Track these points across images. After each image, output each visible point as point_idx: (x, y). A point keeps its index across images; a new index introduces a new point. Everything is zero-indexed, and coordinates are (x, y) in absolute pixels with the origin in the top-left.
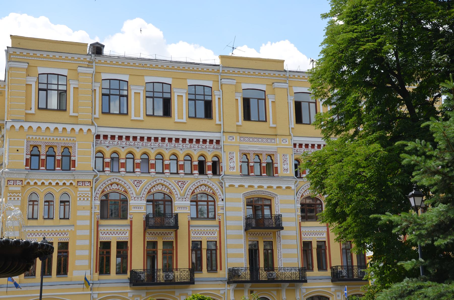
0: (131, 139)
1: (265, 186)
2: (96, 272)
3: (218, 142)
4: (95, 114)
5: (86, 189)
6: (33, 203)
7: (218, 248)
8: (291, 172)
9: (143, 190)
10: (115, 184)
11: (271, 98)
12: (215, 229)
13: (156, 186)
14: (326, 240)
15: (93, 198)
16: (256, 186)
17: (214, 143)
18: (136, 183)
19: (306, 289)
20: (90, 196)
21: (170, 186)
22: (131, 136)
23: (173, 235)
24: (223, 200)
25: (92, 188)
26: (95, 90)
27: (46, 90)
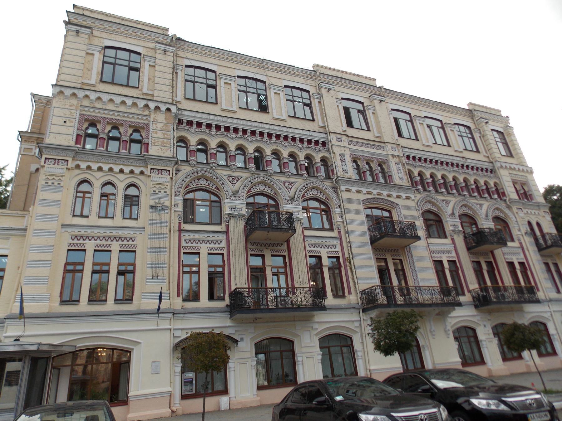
0: (222, 129)
1: (385, 193)
2: (178, 296)
3: (324, 144)
4: (176, 97)
6: (84, 196)
7: (342, 265)
8: (406, 182)
9: (242, 187)
10: (203, 179)
11: (371, 109)
12: (335, 242)
13: (257, 185)
14: (456, 259)
16: (375, 192)
17: (320, 145)
18: (231, 179)
20: (169, 187)
21: (275, 185)
23: (285, 247)
24: (339, 206)
25: (171, 178)
26: (176, 73)
27: (114, 64)
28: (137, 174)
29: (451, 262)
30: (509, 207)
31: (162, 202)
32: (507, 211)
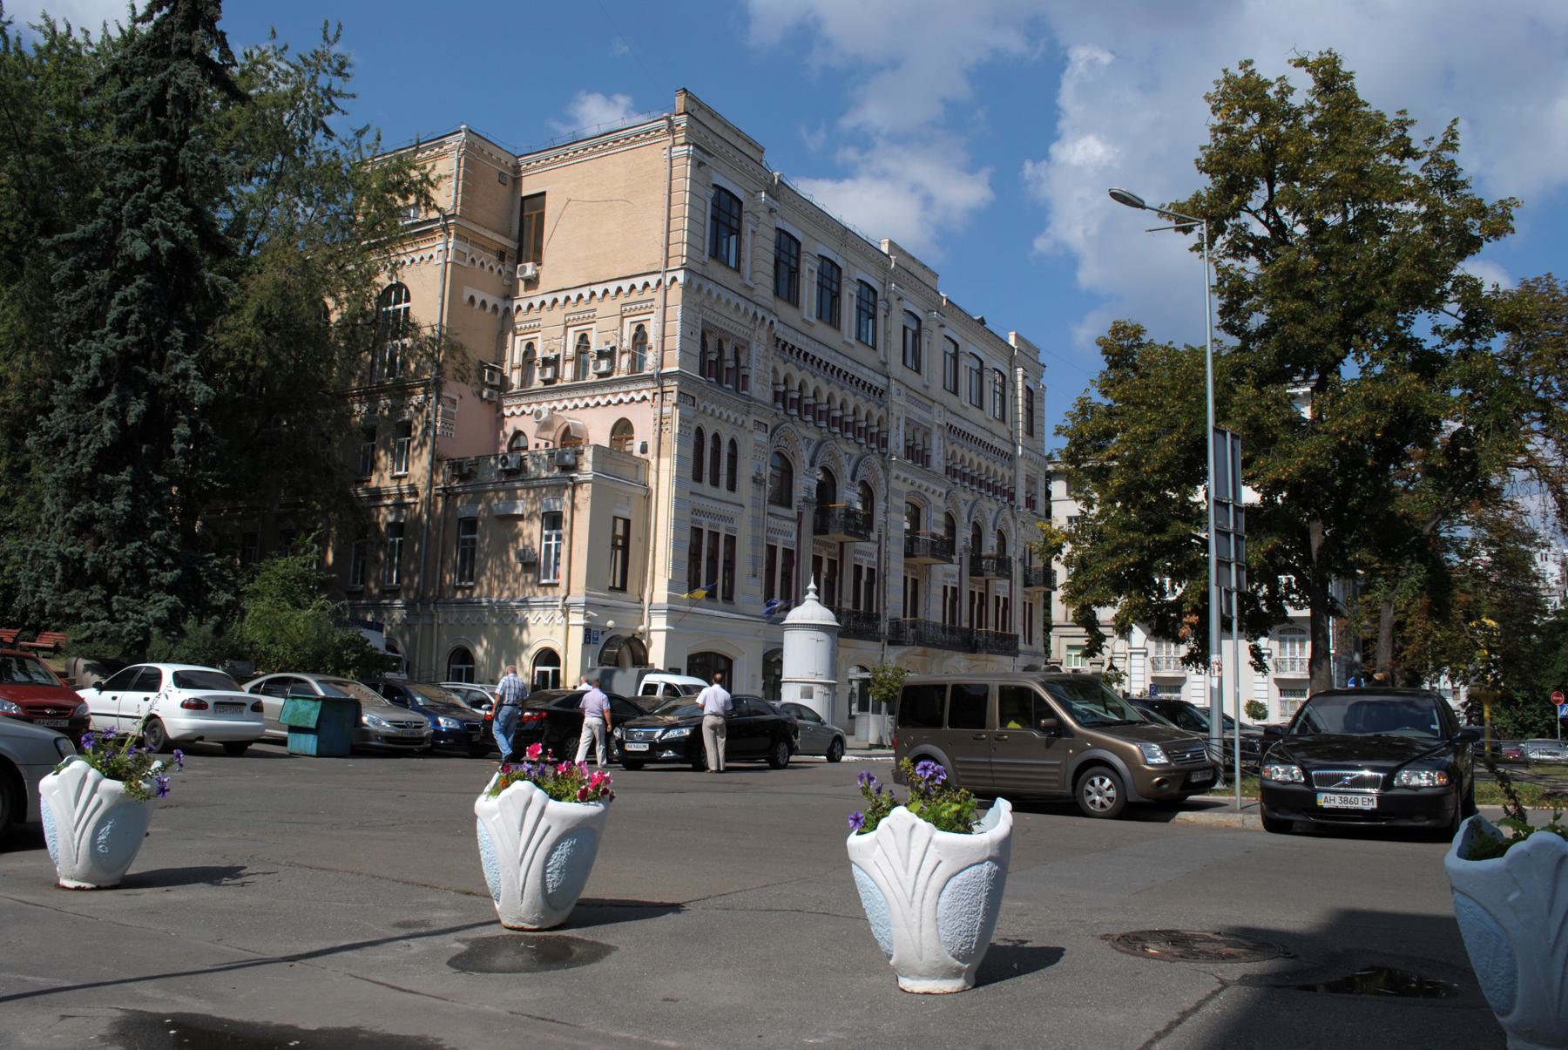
8: (942, 470)
16: (918, 482)
29: (954, 589)
30: (1014, 517)
32: (1011, 523)
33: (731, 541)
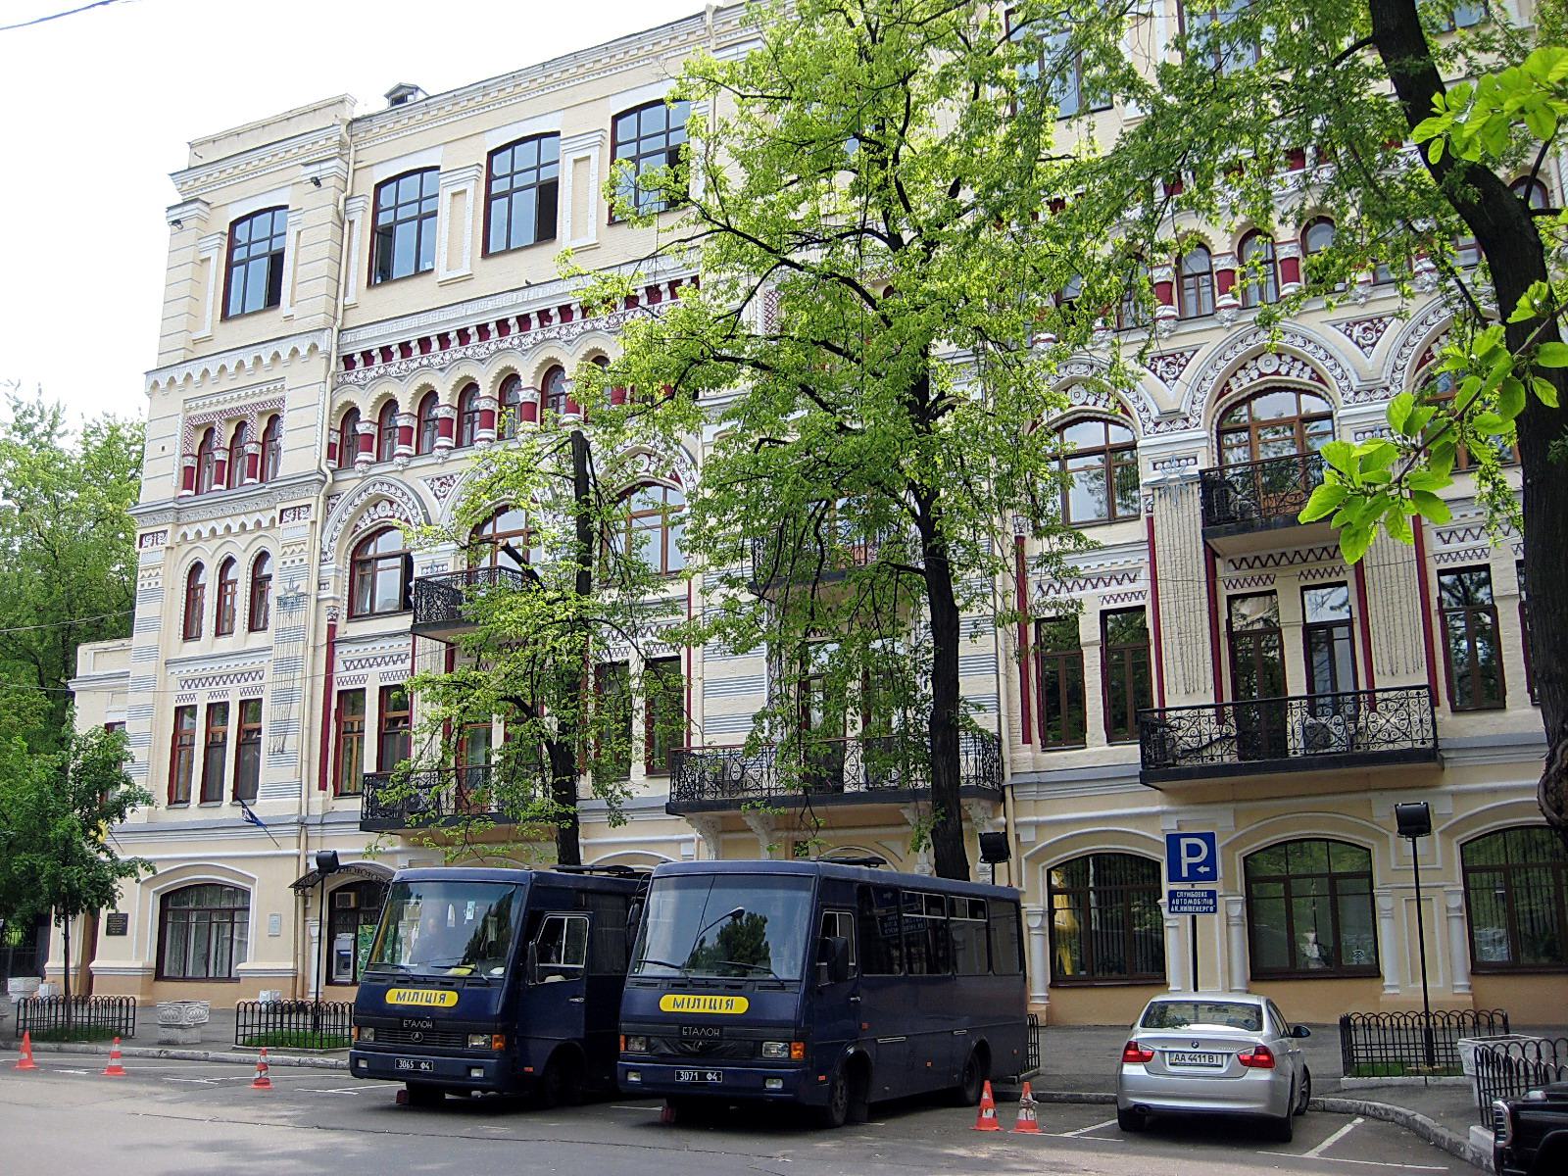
2: (323, 786)
4: (345, 295)
5: (296, 530)
10: (384, 503)
15: (317, 558)
19: (1038, 825)
22: (413, 338)
28: (266, 529)
31: (295, 584)
33: (250, 708)
